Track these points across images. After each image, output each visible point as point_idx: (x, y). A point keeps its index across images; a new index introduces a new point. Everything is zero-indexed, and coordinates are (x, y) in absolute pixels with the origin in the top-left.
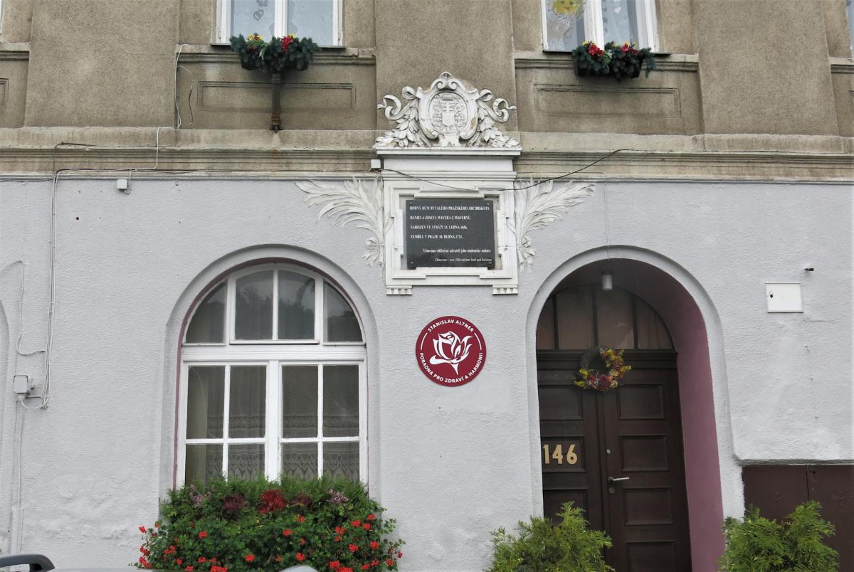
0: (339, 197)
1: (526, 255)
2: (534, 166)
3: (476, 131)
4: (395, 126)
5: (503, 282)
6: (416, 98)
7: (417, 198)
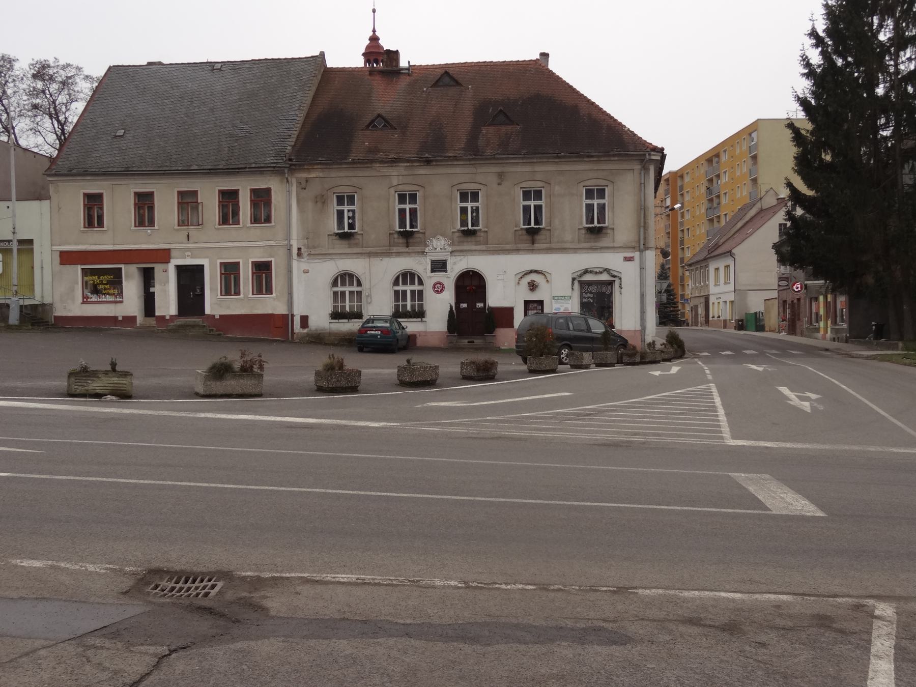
4: (429, 246)
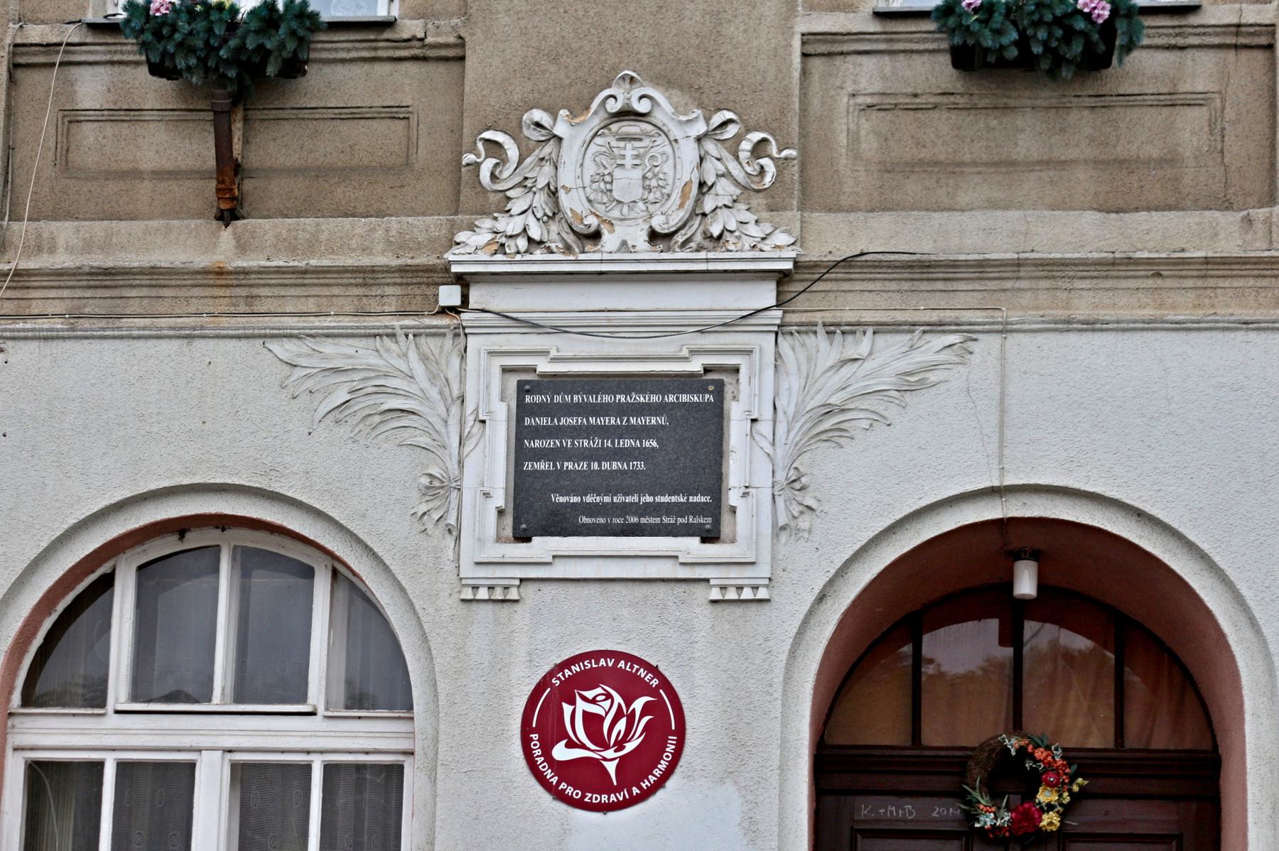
0: (363, 375)
1: (796, 509)
2: (832, 295)
3: (693, 214)
5: (734, 572)
6: (555, 136)
7: (543, 375)
